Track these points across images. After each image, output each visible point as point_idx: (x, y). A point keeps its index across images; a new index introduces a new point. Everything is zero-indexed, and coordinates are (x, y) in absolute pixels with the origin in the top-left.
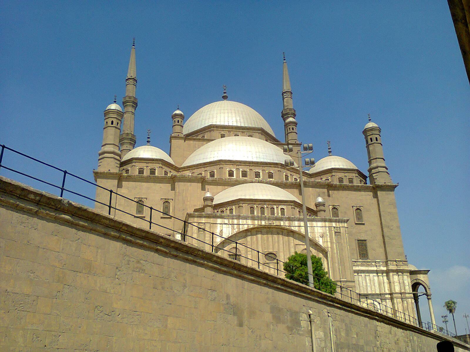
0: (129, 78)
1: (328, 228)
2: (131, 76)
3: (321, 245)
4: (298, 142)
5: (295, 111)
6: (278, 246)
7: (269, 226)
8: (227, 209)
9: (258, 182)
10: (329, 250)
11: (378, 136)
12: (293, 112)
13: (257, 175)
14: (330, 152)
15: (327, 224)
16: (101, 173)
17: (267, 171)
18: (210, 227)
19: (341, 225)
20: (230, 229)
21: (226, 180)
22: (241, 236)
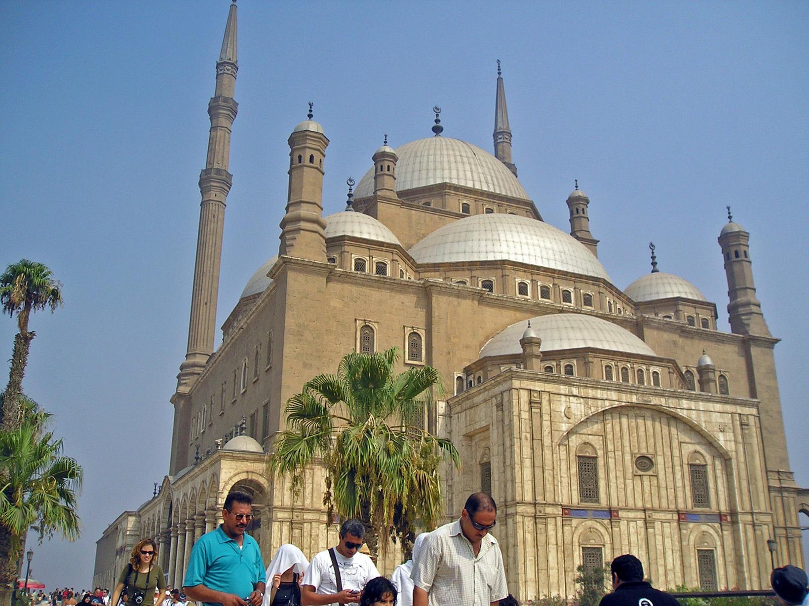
0: (225, 63)
8: (558, 365)
11: (744, 248)
13: (567, 297)
14: (654, 264)
15: (729, 408)
16: (296, 263)
18: (550, 401)
19: (746, 410)
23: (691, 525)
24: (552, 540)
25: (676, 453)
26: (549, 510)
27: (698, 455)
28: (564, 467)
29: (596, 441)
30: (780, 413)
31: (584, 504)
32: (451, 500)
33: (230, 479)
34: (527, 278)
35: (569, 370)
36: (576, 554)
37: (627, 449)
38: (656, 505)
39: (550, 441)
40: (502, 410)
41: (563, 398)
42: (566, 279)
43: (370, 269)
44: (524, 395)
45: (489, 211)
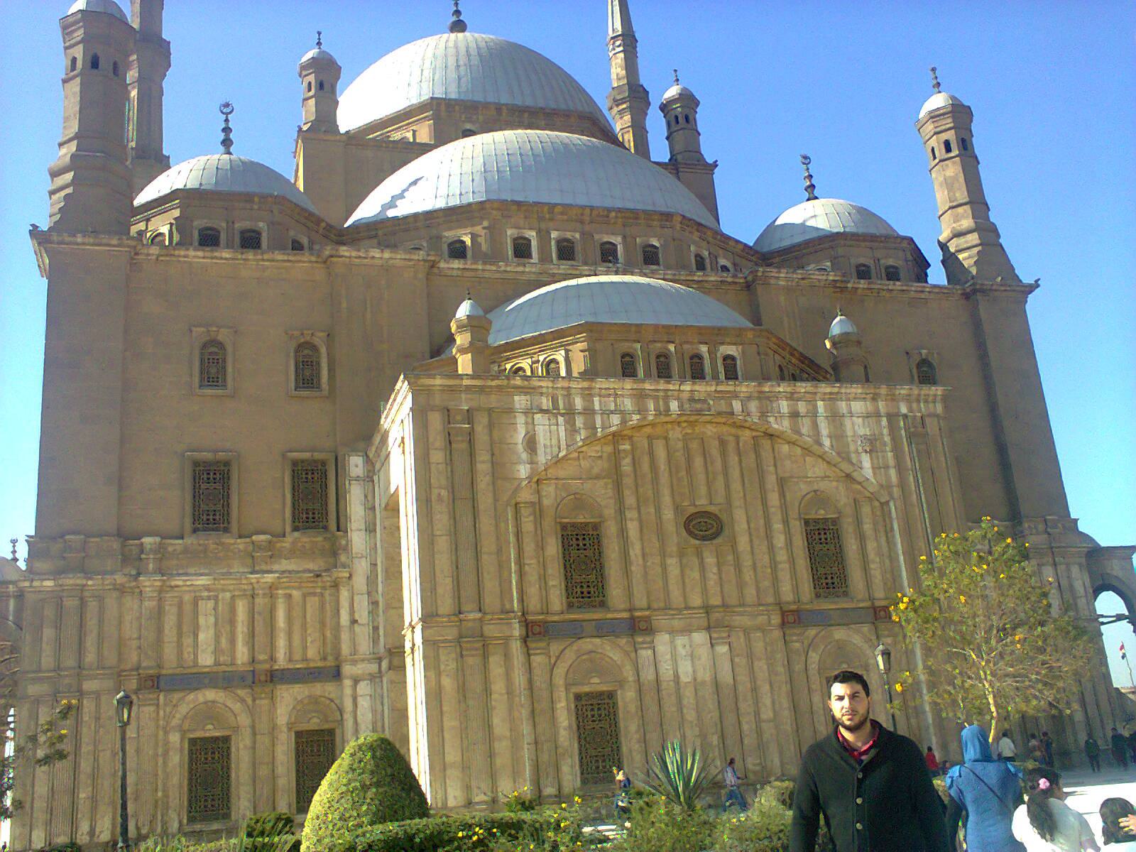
1: (884, 421)
5: (647, 93)
6: (727, 487)
18: (491, 426)
20: (562, 429)
21: (508, 269)
22: (599, 454)
23: (812, 632)
24: (498, 687)
25: (774, 499)
26: (490, 630)
28: (529, 547)
29: (601, 493)
32: (376, 629)
34: (531, 229)
36: (561, 705)
37: (667, 499)
38: (733, 600)
39: (490, 500)
41: (521, 419)
42: (607, 223)
44: (436, 420)
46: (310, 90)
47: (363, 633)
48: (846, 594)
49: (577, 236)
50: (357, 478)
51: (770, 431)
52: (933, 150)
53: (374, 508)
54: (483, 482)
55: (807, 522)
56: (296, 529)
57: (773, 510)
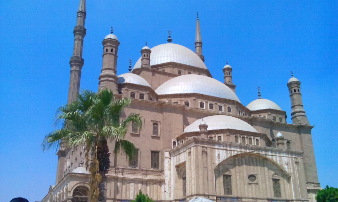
0: (80, 12)
2: (82, 10)
3: (286, 171)
4: (234, 85)
5: (204, 58)
7: (250, 153)
8: (216, 136)
9: (222, 114)
10: (292, 176)
11: (299, 89)
12: (203, 58)
13: (220, 108)
14: (259, 95)
17: (227, 106)
18: (211, 151)
20: (225, 154)
25: (267, 173)
27: (276, 175)
30: (314, 158)
31: (226, 195)
32: (170, 194)
33: (74, 186)
35: (220, 138)
38: (258, 197)
40: (190, 155)
41: (217, 150)
43: (137, 96)
45: (189, 73)
46: (144, 56)
47: (167, 194)
48: (281, 197)
49: (214, 104)
50: (167, 157)
51: (266, 158)
52: (291, 91)
53: (170, 165)
54: (209, 164)
55: (273, 180)
56: (152, 168)
57: (266, 176)
